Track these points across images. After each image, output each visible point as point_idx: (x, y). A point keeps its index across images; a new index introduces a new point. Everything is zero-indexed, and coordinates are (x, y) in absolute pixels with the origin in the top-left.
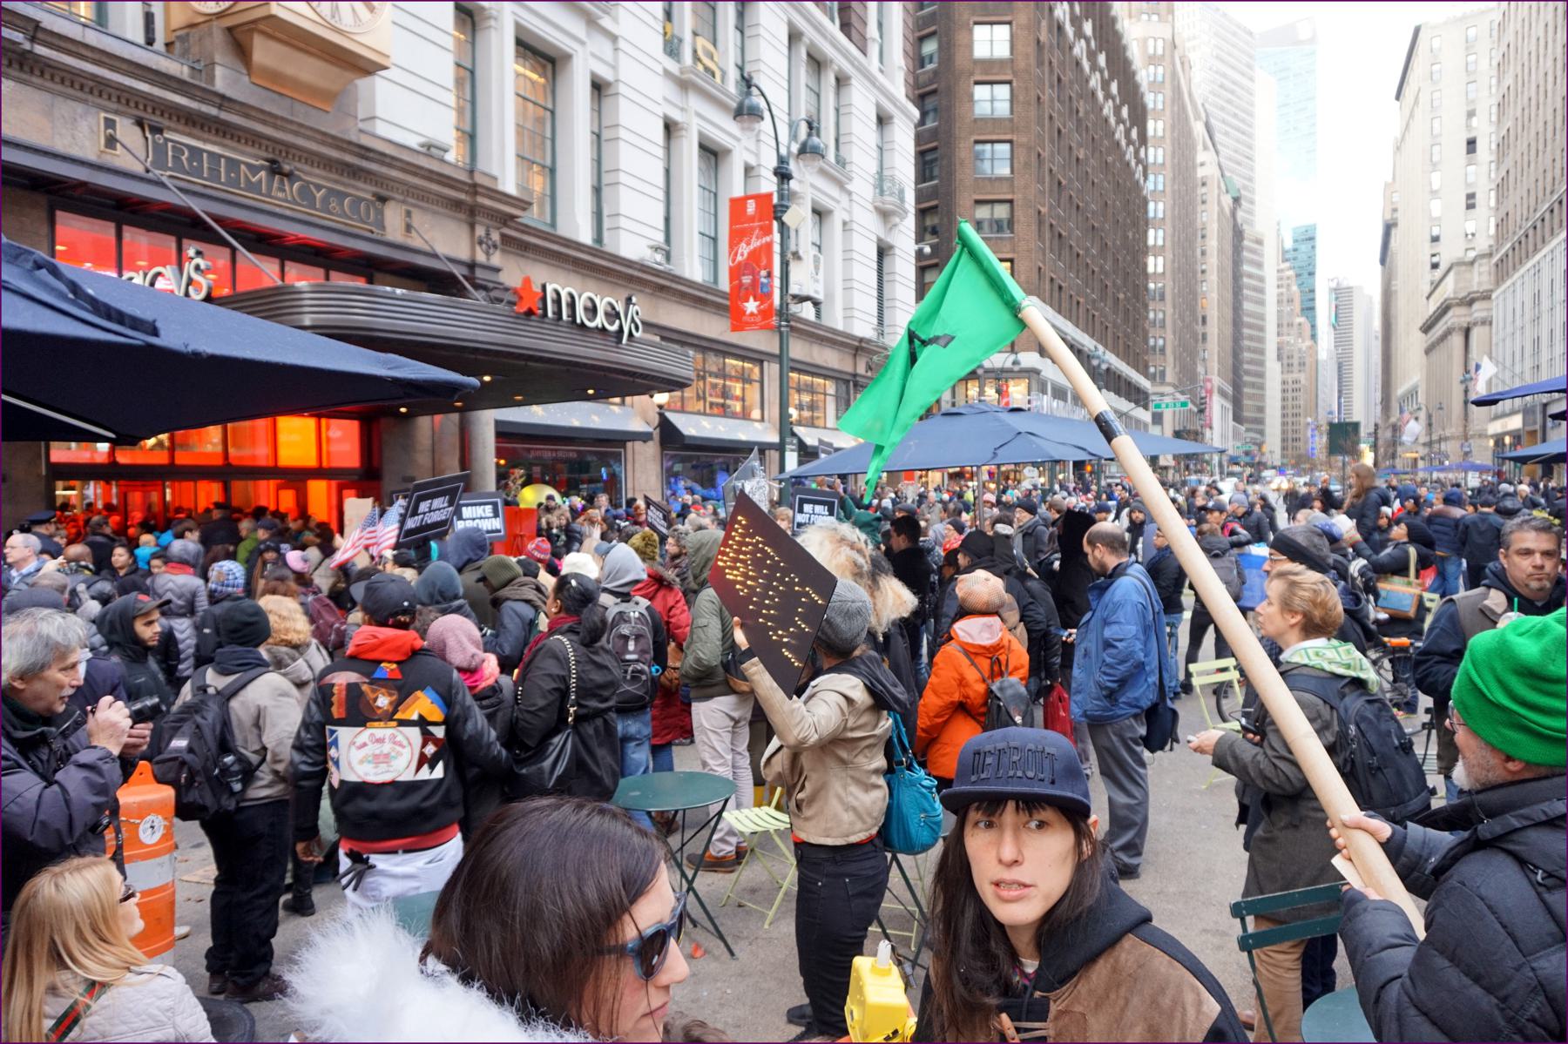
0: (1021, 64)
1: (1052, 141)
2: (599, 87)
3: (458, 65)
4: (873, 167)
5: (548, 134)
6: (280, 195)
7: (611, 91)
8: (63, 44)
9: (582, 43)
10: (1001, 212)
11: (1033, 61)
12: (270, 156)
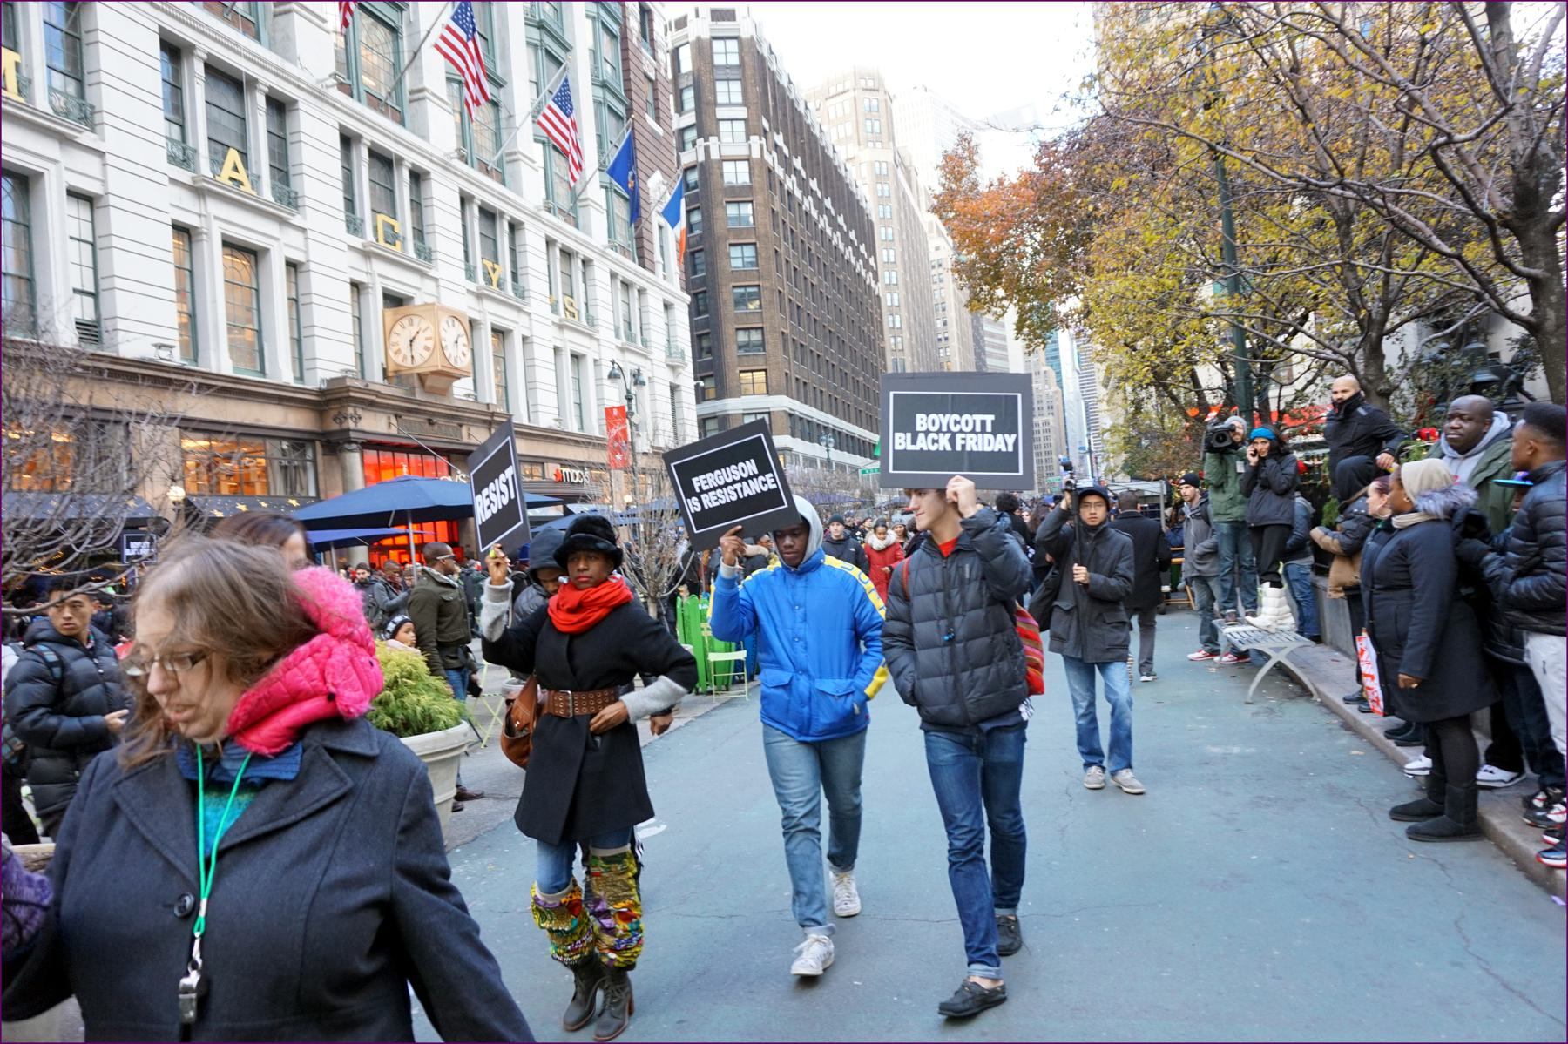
0: (762, 230)
1: (789, 279)
2: (524, 338)
10: (756, 337)
11: (770, 228)
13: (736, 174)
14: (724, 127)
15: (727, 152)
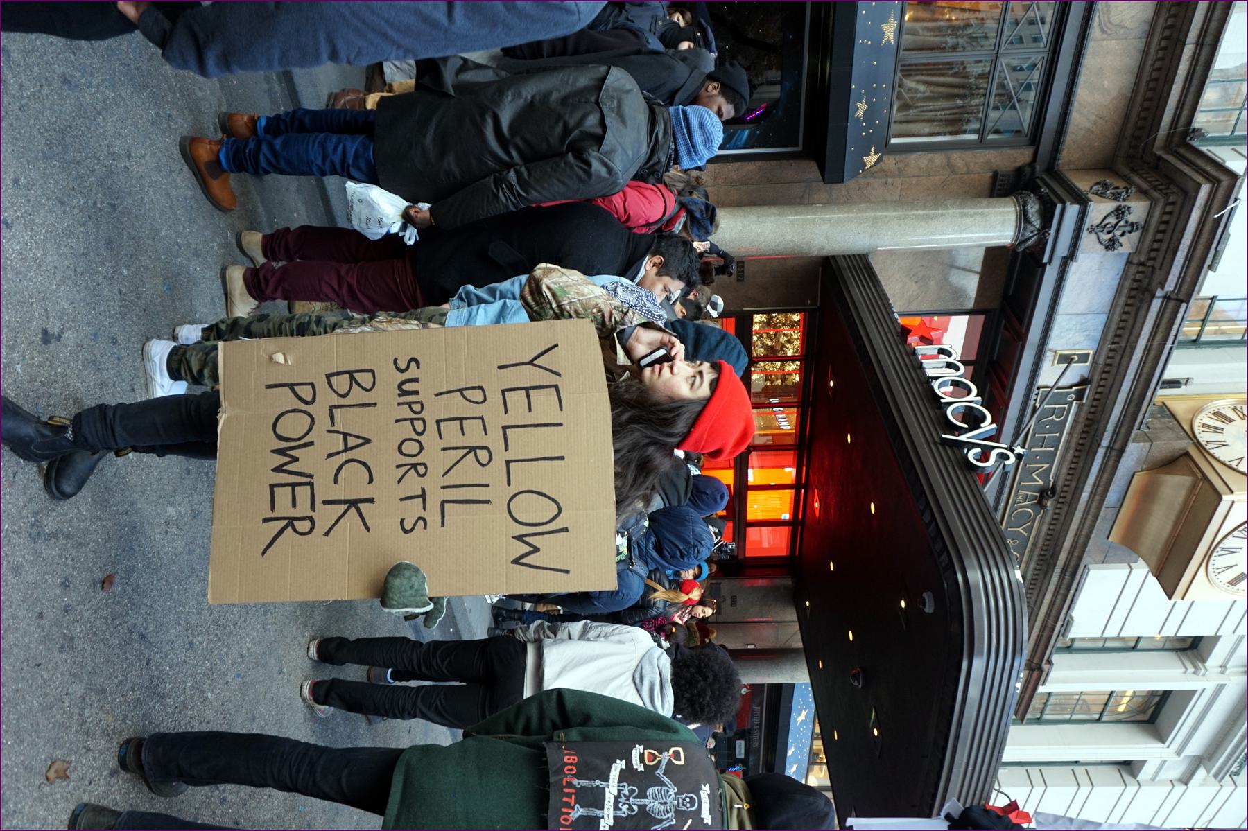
2: (1129, 768)
3: (1139, 639)
5: (1074, 717)
6: (1020, 497)
7: (1128, 778)
8: (1165, 321)
9: (1179, 753)
12: (1058, 489)
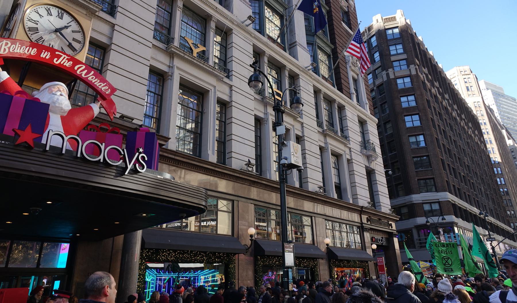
4: (360, 139)
13: (403, 83)
14: (395, 64)
15: (397, 74)
